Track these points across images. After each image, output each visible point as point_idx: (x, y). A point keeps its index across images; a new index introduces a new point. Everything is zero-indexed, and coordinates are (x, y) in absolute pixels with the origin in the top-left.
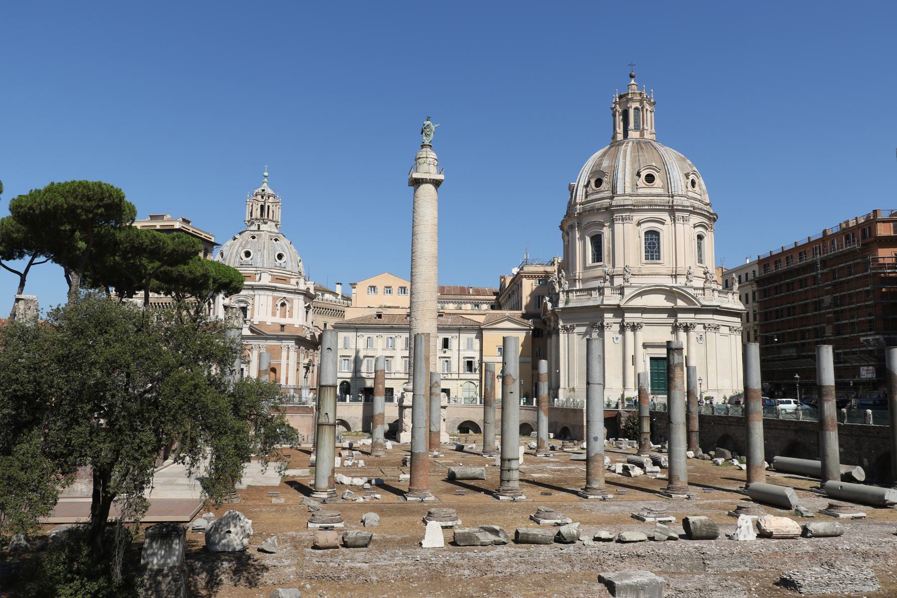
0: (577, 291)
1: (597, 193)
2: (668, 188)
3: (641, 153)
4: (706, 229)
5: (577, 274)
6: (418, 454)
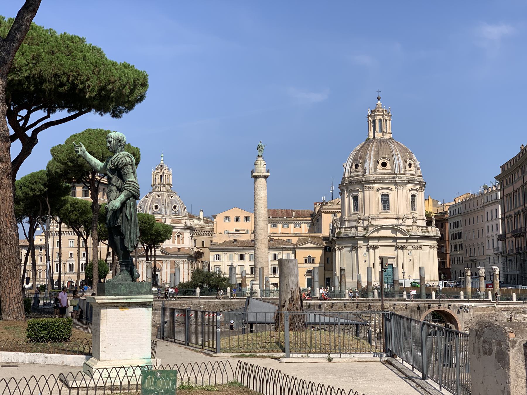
0: (345, 228)
3: (380, 149)
4: (418, 191)
5: (346, 218)
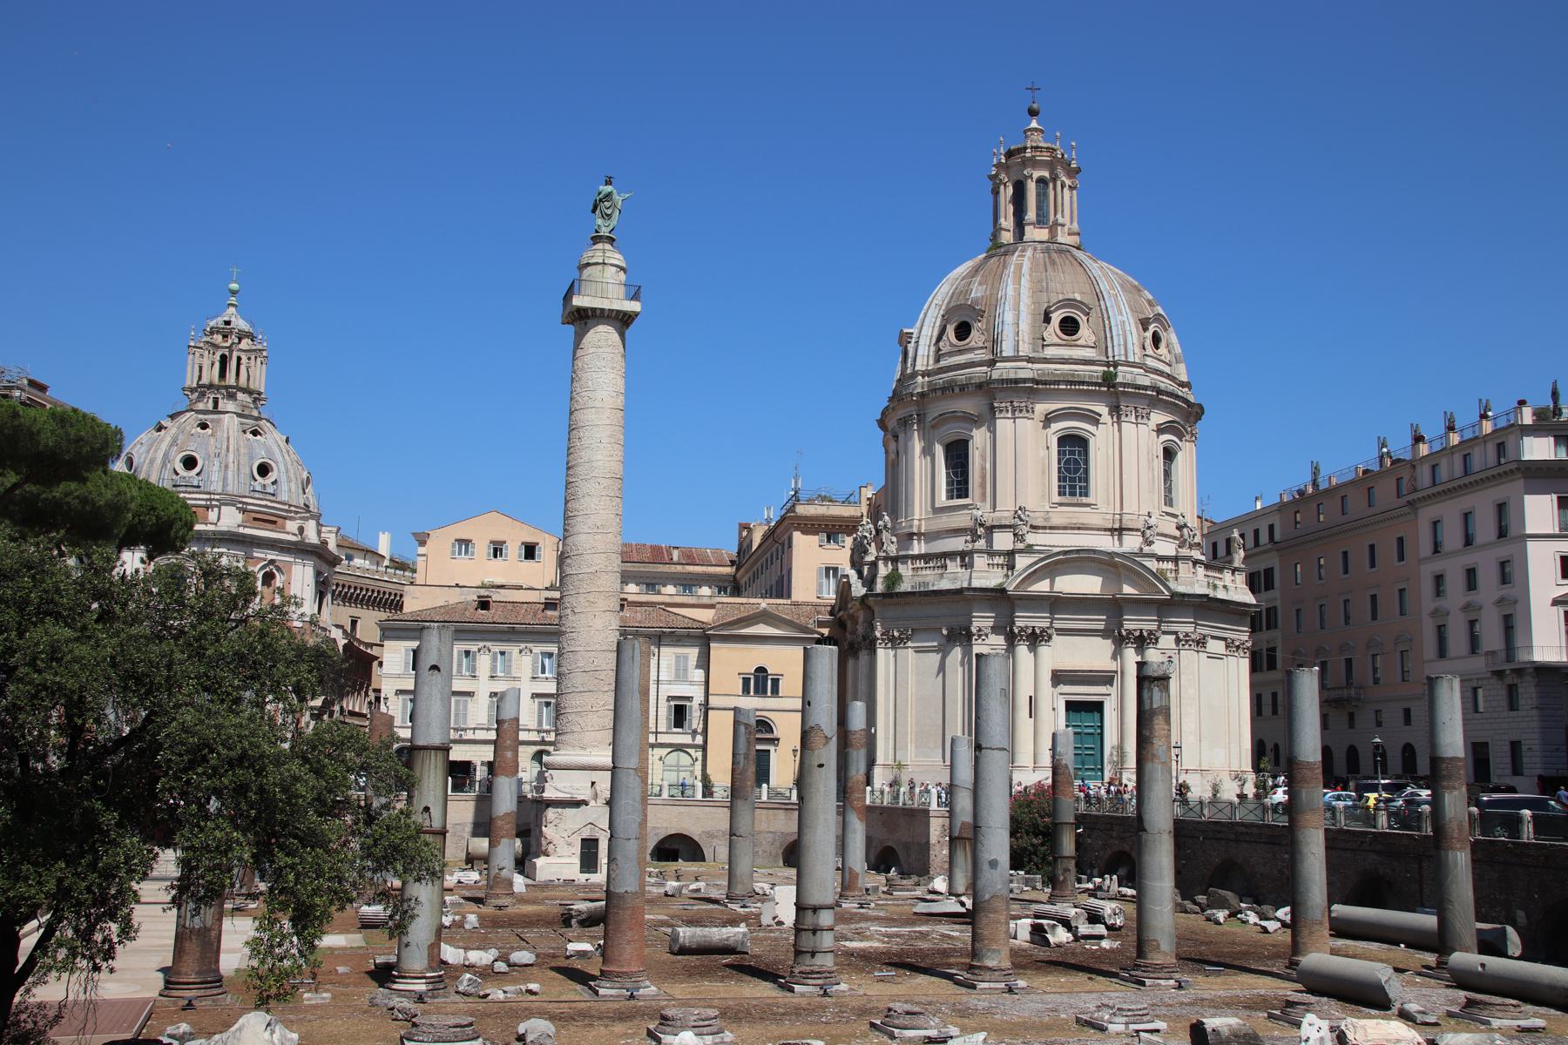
0: (914, 558)
1: (961, 352)
2: (1107, 348)
4: (1181, 437)
5: (916, 523)
6: (621, 897)
